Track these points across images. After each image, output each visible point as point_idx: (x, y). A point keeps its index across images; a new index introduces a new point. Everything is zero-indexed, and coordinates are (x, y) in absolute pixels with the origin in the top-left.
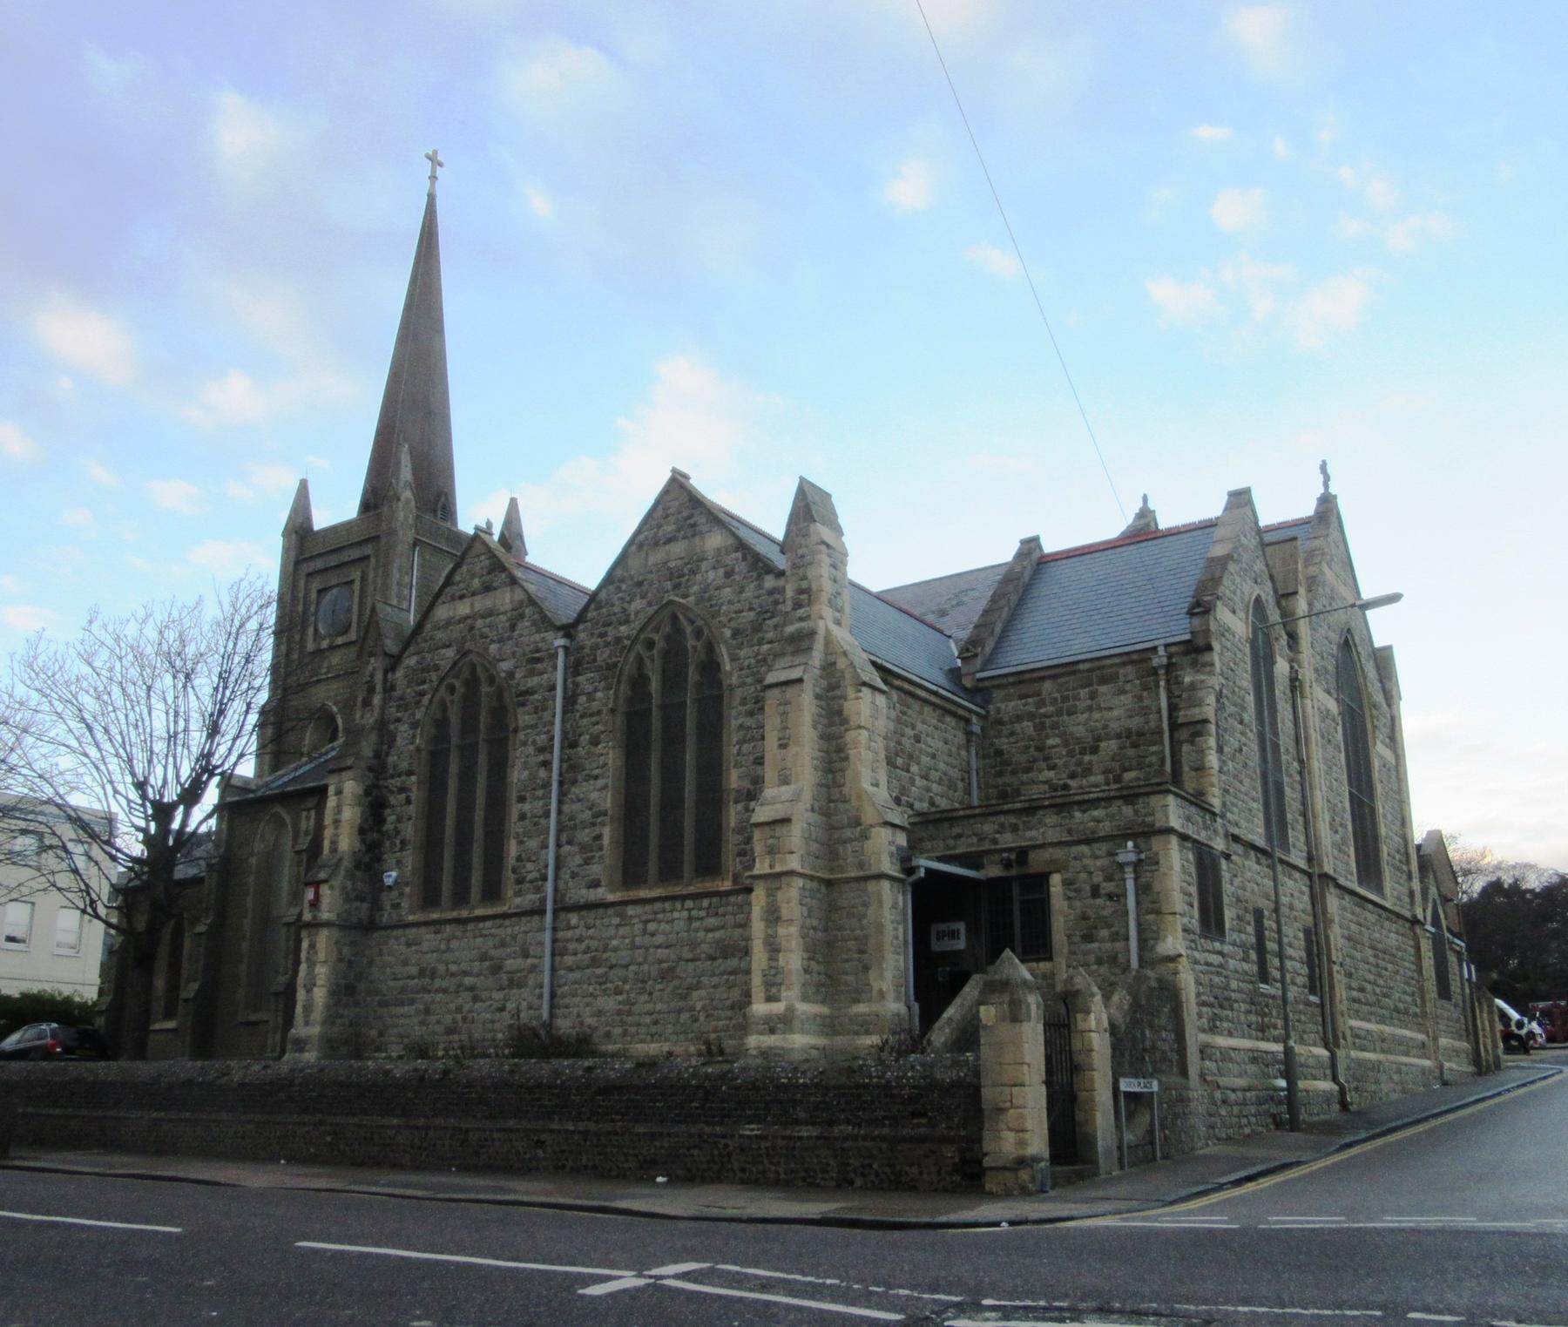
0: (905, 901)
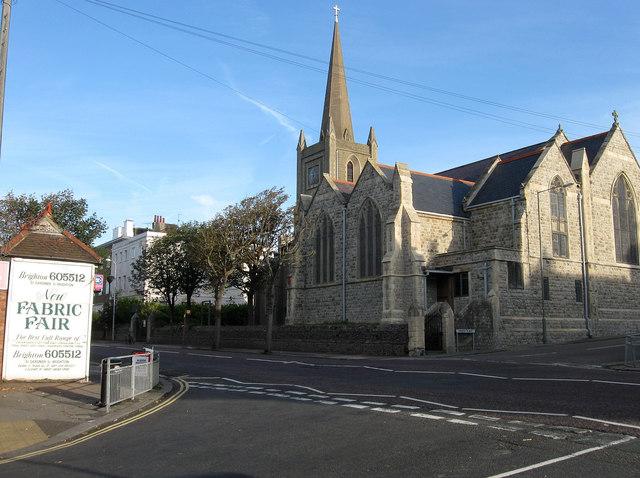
0: (424, 281)
